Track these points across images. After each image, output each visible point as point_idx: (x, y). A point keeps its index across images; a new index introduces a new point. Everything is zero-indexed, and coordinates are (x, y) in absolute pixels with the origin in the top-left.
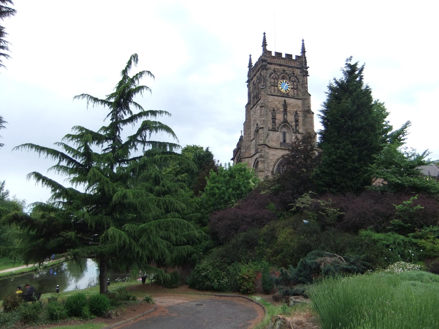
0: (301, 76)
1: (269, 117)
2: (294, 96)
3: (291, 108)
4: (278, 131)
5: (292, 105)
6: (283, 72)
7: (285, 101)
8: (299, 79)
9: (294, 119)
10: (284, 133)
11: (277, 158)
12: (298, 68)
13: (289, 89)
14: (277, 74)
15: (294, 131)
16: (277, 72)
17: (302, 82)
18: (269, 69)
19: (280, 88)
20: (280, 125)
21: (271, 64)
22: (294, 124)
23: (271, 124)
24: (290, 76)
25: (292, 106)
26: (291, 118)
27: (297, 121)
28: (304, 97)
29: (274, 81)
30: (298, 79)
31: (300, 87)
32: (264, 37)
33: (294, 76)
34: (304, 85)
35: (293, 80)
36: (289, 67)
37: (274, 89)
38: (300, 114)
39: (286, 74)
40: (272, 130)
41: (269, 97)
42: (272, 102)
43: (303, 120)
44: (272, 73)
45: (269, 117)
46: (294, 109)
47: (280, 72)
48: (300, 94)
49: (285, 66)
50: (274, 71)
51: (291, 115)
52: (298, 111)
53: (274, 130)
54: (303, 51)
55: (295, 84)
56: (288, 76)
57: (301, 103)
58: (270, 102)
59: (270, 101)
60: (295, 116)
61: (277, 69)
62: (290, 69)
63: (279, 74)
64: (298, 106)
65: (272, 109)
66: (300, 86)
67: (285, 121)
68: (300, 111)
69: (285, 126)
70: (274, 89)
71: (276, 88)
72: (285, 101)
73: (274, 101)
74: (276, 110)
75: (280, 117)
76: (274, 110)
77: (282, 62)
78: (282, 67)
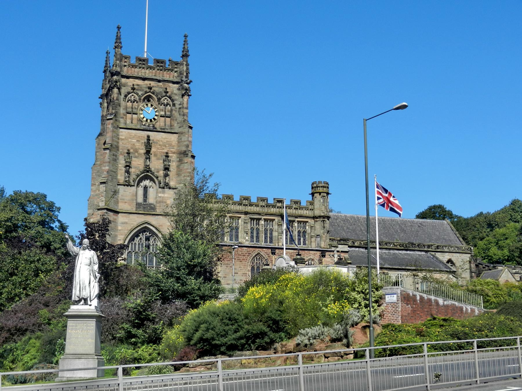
0: (179, 95)
1: (120, 164)
2: (164, 129)
3: (158, 149)
4: (134, 186)
5: (161, 143)
6: (148, 90)
7: (148, 137)
8: (176, 100)
9: (163, 165)
10: (146, 188)
11: (129, 228)
12: (174, 83)
13: (156, 118)
14: (137, 94)
16: (137, 90)
17: (180, 104)
18: (125, 85)
19: (142, 116)
21: (128, 77)
22: (161, 173)
23: (123, 174)
24: (159, 96)
25: (160, 145)
26: (156, 165)
27: (167, 169)
28: (180, 130)
29: (132, 105)
30: (173, 101)
31: (176, 114)
33: (167, 96)
34: (181, 110)
35: (166, 102)
36: (159, 81)
37: (132, 119)
38: (174, 157)
39: (153, 93)
40: (124, 185)
41: (122, 132)
42: (126, 139)
43: (178, 167)
44: (129, 93)
45: (120, 164)
46: (163, 149)
47: (143, 90)
48: (176, 125)
50: (133, 89)
51: (158, 159)
52: (169, 152)
53: (127, 184)
55: (168, 107)
56: (157, 96)
57: (176, 140)
58: (122, 139)
59: (123, 137)
60: (164, 161)
61: (138, 85)
62: (161, 84)
63: (140, 93)
64: (170, 145)
65: (126, 151)
66: (176, 111)
67: (147, 169)
68: (174, 153)
69: (146, 178)
70: (132, 119)
71: (135, 116)
72: (148, 136)
73: (130, 138)
74: (132, 153)
75: (138, 164)
76: (128, 153)
77: (148, 73)
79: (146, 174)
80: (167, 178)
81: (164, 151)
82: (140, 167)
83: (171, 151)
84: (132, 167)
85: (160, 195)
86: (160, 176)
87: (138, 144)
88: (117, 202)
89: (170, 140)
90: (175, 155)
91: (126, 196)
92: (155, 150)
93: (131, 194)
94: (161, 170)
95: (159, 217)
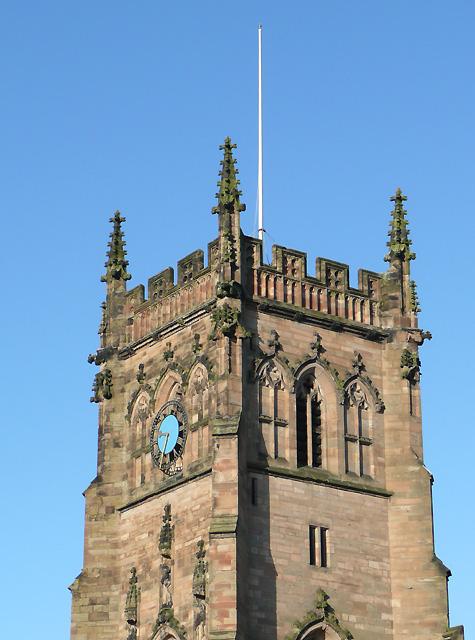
2: (196, 469)
21: (129, 352)
32: (117, 234)
39: (173, 367)
42: (131, 539)
54: (229, 205)
58: (125, 544)
59: (125, 537)
63: (152, 382)
67: (166, 616)
72: (168, 508)
76: (134, 580)
78: (164, 343)
84: (142, 621)
87: (151, 544)
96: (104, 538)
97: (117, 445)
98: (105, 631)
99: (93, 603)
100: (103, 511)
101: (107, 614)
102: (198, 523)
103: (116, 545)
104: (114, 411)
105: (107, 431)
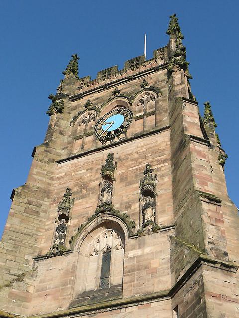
1: (49, 219)
4: (69, 252)
5: (136, 156)
7: (110, 156)
15: (138, 228)
20: (80, 229)
21: (79, 97)
25: (132, 160)
39: (122, 97)
46: (141, 163)
49: (120, 82)
53: (59, 252)
58: (59, 178)
72: (110, 156)
75: (85, 206)
76: (68, 193)
79: (100, 219)
80: (149, 211)
81: (141, 166)
82: (89, 212)
83: (158, 161)
84: (73, 216)
85: (131, 254)
86: (134, 214)
88: (25, 298)
89: (154, 144)
90: (167, 164)
91: (52, 280)
92: (123, 171)
93: (62, 272)
94: (134, 202)
95: (129, 309)
96: (45, 173)
97: (61, 133)
98: (35, 222)
99: (29, 203)
100: (47, 159)
101: (38, 213)
102: (146, 157)
103: (52, 179)
104: (62, 119)
105: (57, 126)
